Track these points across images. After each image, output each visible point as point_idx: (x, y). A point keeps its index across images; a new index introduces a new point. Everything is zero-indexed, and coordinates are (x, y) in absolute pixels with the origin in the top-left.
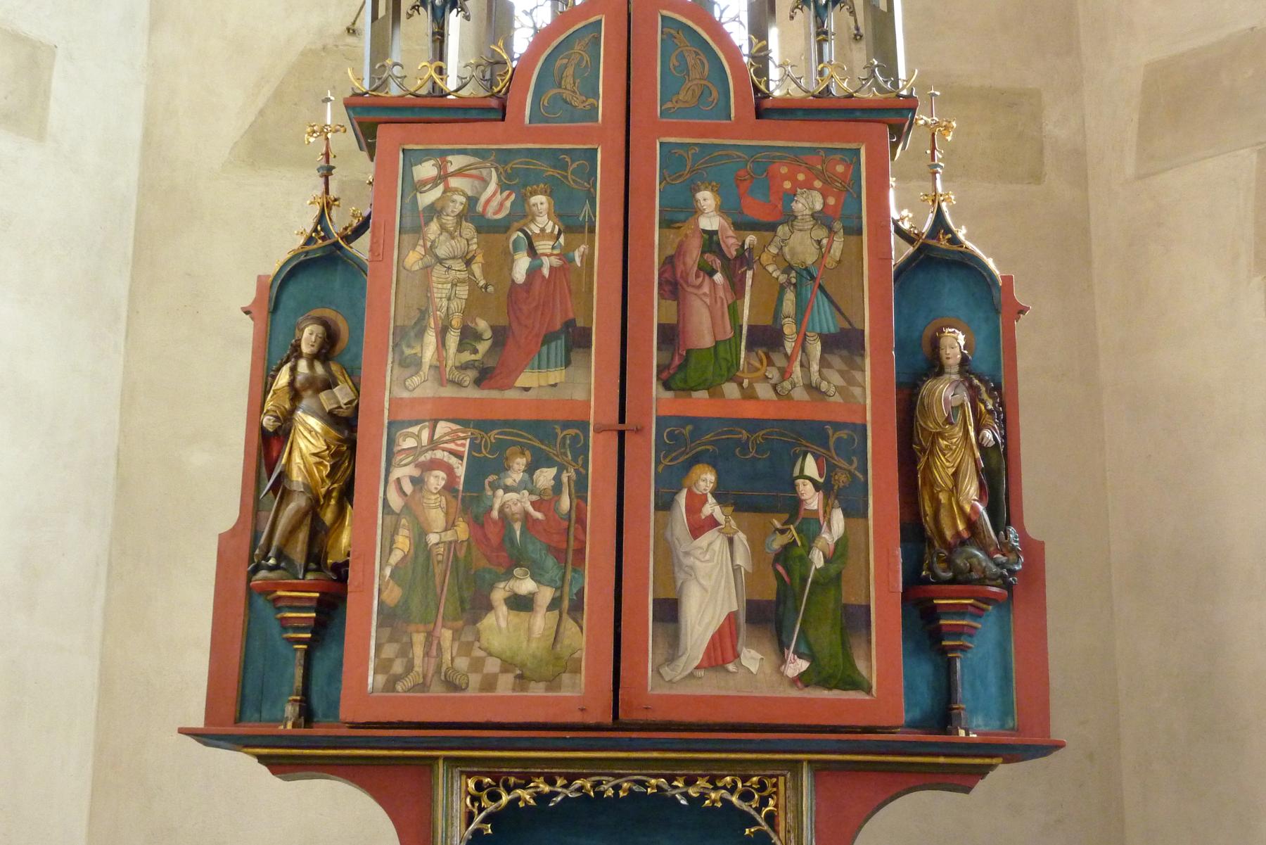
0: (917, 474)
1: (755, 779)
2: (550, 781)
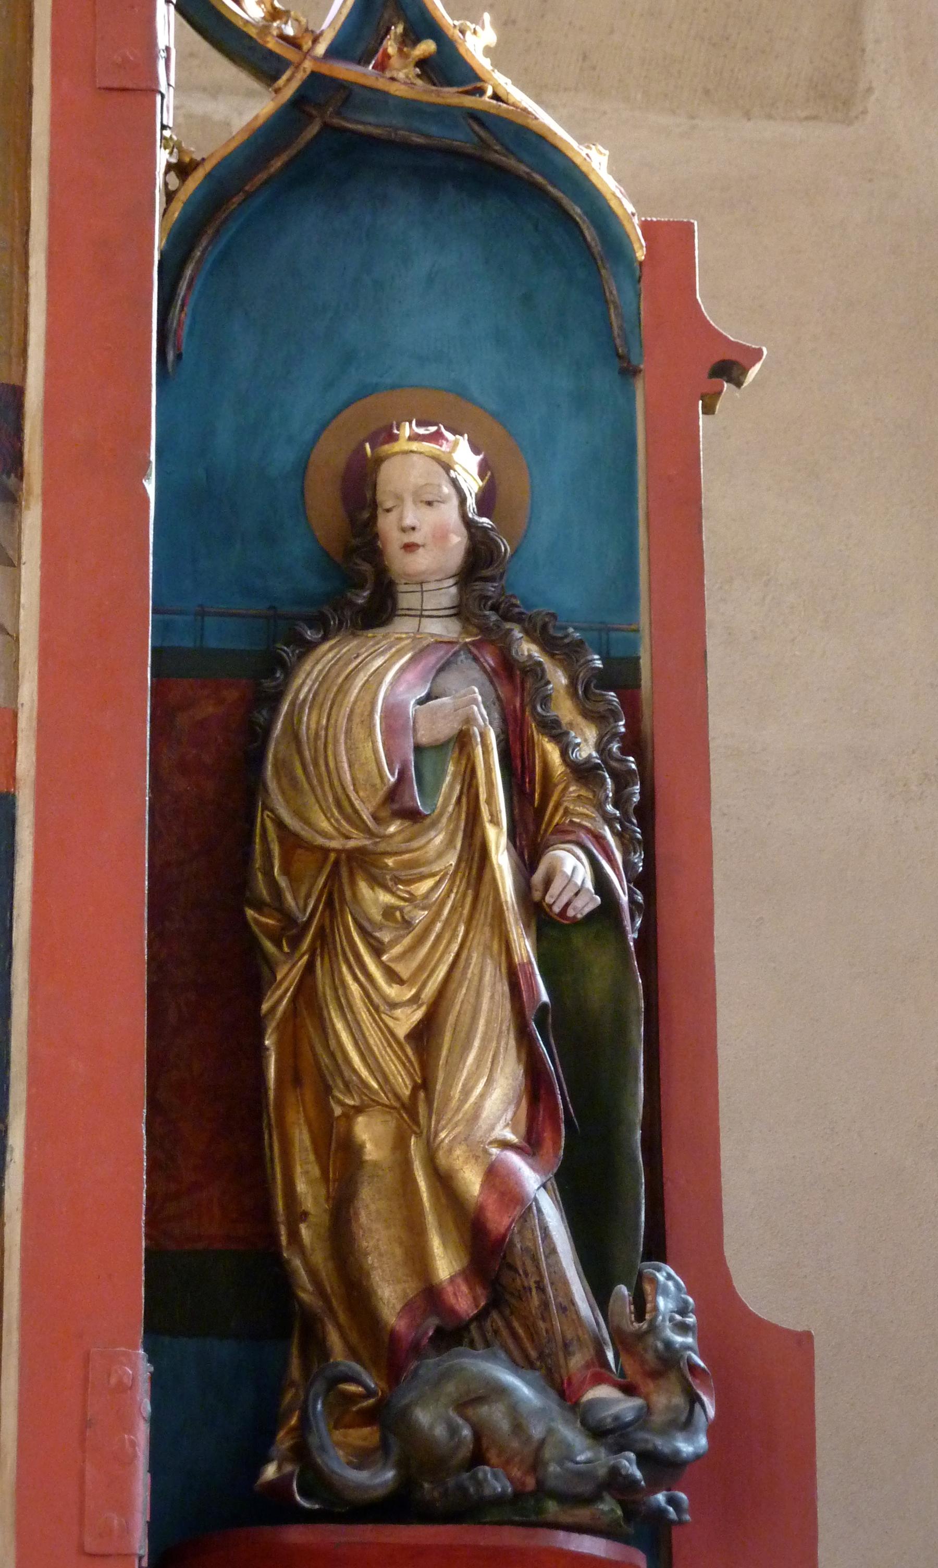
0: (261, 1036)
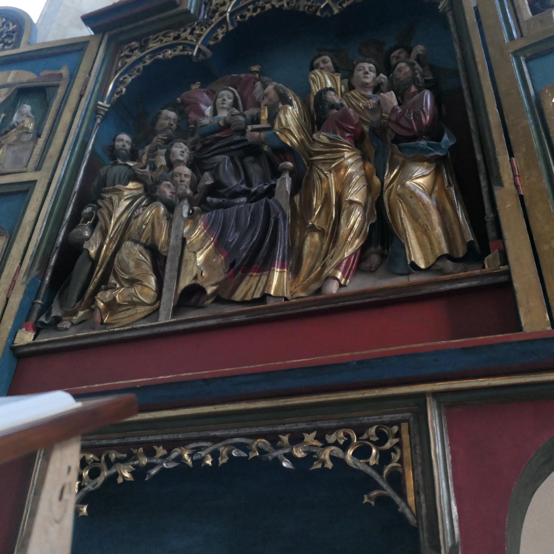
1: (373, 430)
2: (150, 453)
